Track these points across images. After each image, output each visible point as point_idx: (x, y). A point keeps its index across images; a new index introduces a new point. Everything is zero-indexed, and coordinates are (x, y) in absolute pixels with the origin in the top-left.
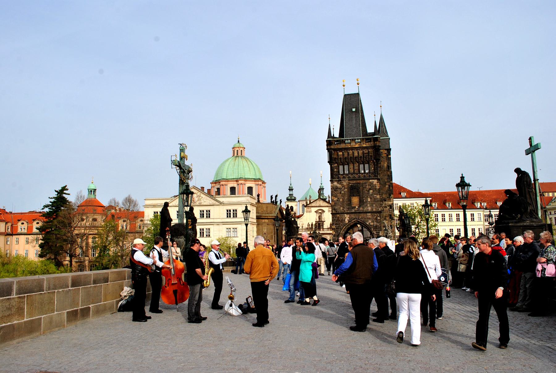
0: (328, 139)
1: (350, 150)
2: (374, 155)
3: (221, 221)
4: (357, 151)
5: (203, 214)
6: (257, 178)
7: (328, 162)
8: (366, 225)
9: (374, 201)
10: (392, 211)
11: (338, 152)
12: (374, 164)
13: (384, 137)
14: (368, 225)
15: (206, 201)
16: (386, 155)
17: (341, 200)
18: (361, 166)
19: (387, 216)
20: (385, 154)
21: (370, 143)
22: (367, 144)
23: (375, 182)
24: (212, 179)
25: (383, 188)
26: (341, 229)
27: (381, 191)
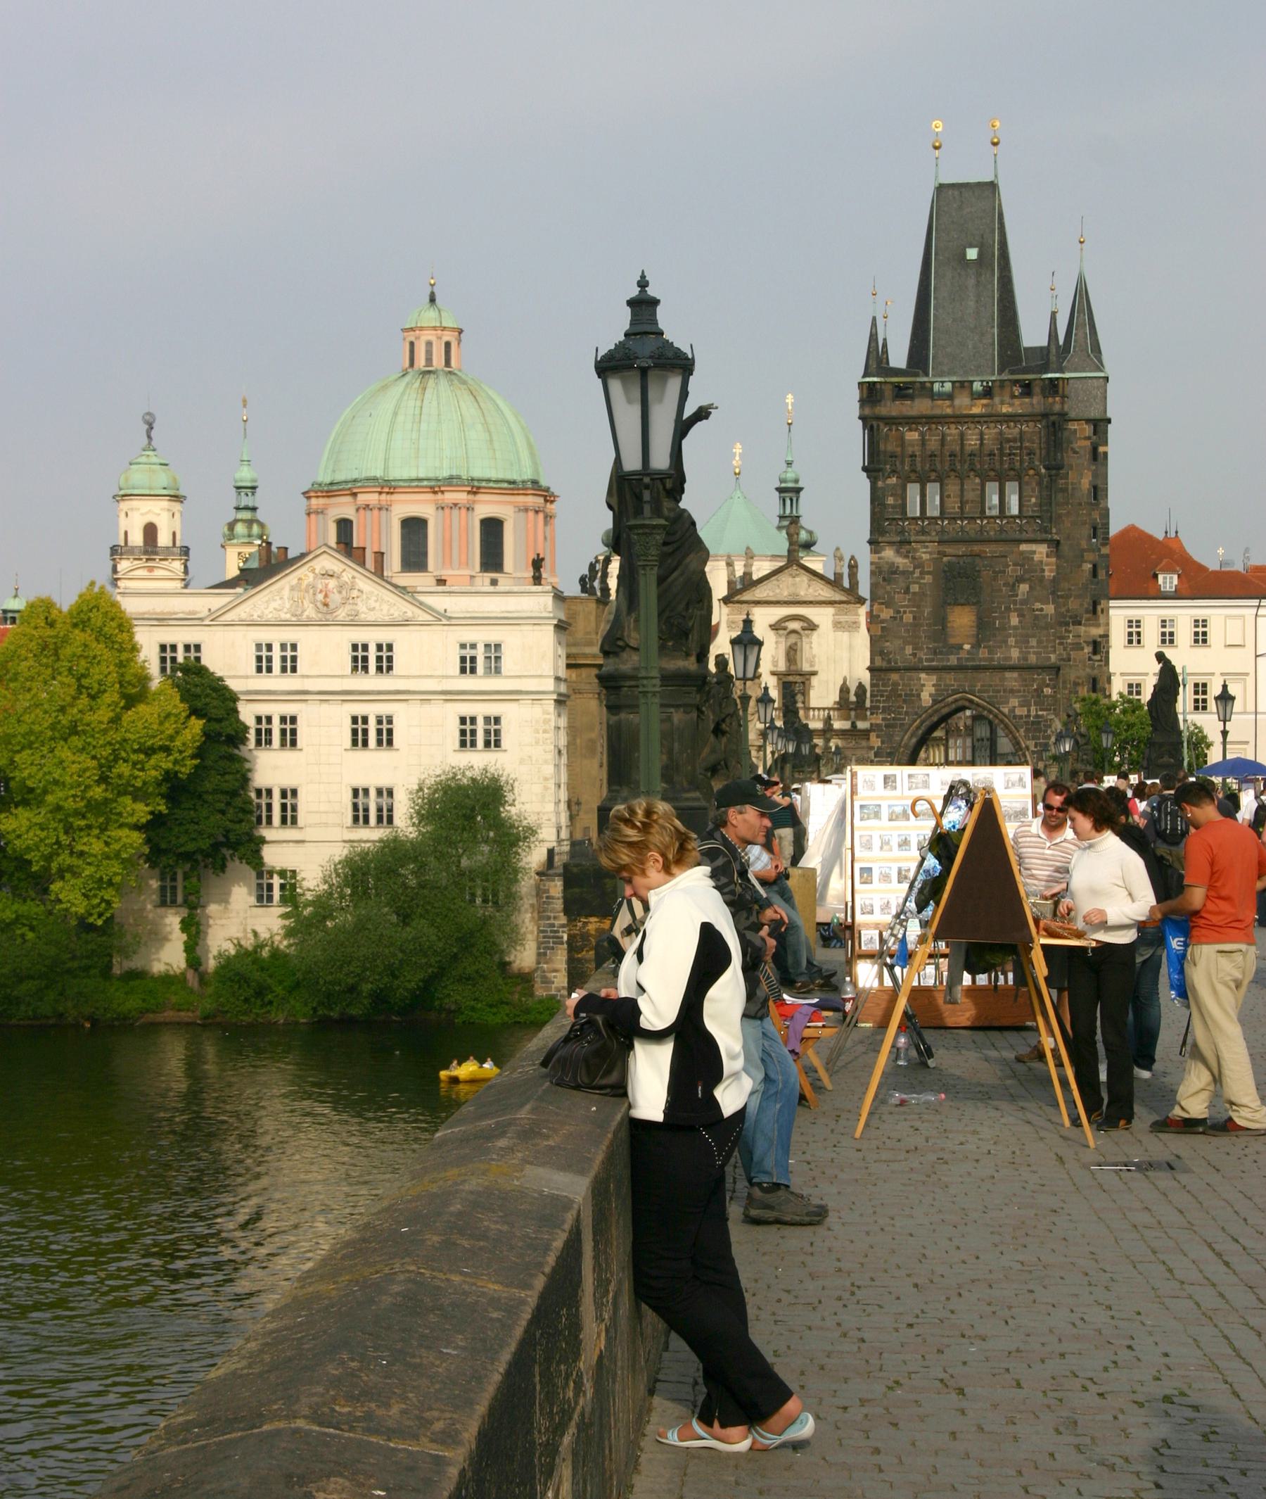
0: (864, 376)
2: (1041, 448)
3: (439, 689)
5: (365, 659)
6: (525, 477)
7: (865, 469)
8: (1001, 716)
10: (1103, 663)
11: (903, 433)
12: (1040, 483)
13: (1084, 371)
14: (1005, 715)
16: (1088, 443)
17: (908, 618)
19: (1080, 681)
20: (1089, 438)
21: (1027, 400)
22: (1017, 402)
23: (1041, 553)
25: (1071, 572)
26: (907, 727)
27: (1065, 585)
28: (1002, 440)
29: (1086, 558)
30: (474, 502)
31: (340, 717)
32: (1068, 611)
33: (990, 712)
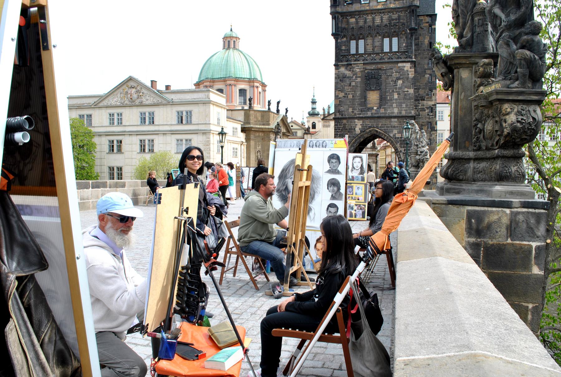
1: (369, 14)
2: (407, 22)
4: (380, 16)
5: (145, 119)
6: (253, 77)
7: (333, 35)
9: (405, 99)
12: (406, 37)
14: (391, 137)
15: (149, 98)
16: (427, 24)
17: (350, 96)
18: (386, 41)
22: (397, 2)
23: (407, 67)
24: (196, 80)
25: (420, 78)
28: (390, 20)
29: (427, 73)
30: (237, 84)
31: (136, 140)
32: (419, 95)
33: (385, 135)
